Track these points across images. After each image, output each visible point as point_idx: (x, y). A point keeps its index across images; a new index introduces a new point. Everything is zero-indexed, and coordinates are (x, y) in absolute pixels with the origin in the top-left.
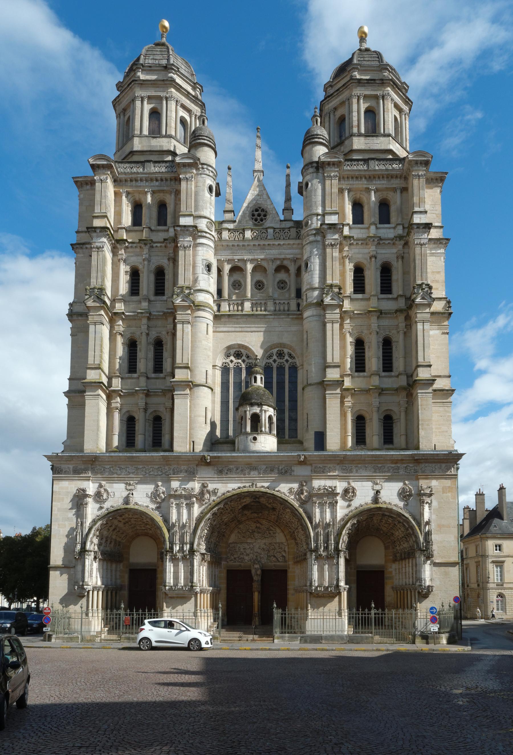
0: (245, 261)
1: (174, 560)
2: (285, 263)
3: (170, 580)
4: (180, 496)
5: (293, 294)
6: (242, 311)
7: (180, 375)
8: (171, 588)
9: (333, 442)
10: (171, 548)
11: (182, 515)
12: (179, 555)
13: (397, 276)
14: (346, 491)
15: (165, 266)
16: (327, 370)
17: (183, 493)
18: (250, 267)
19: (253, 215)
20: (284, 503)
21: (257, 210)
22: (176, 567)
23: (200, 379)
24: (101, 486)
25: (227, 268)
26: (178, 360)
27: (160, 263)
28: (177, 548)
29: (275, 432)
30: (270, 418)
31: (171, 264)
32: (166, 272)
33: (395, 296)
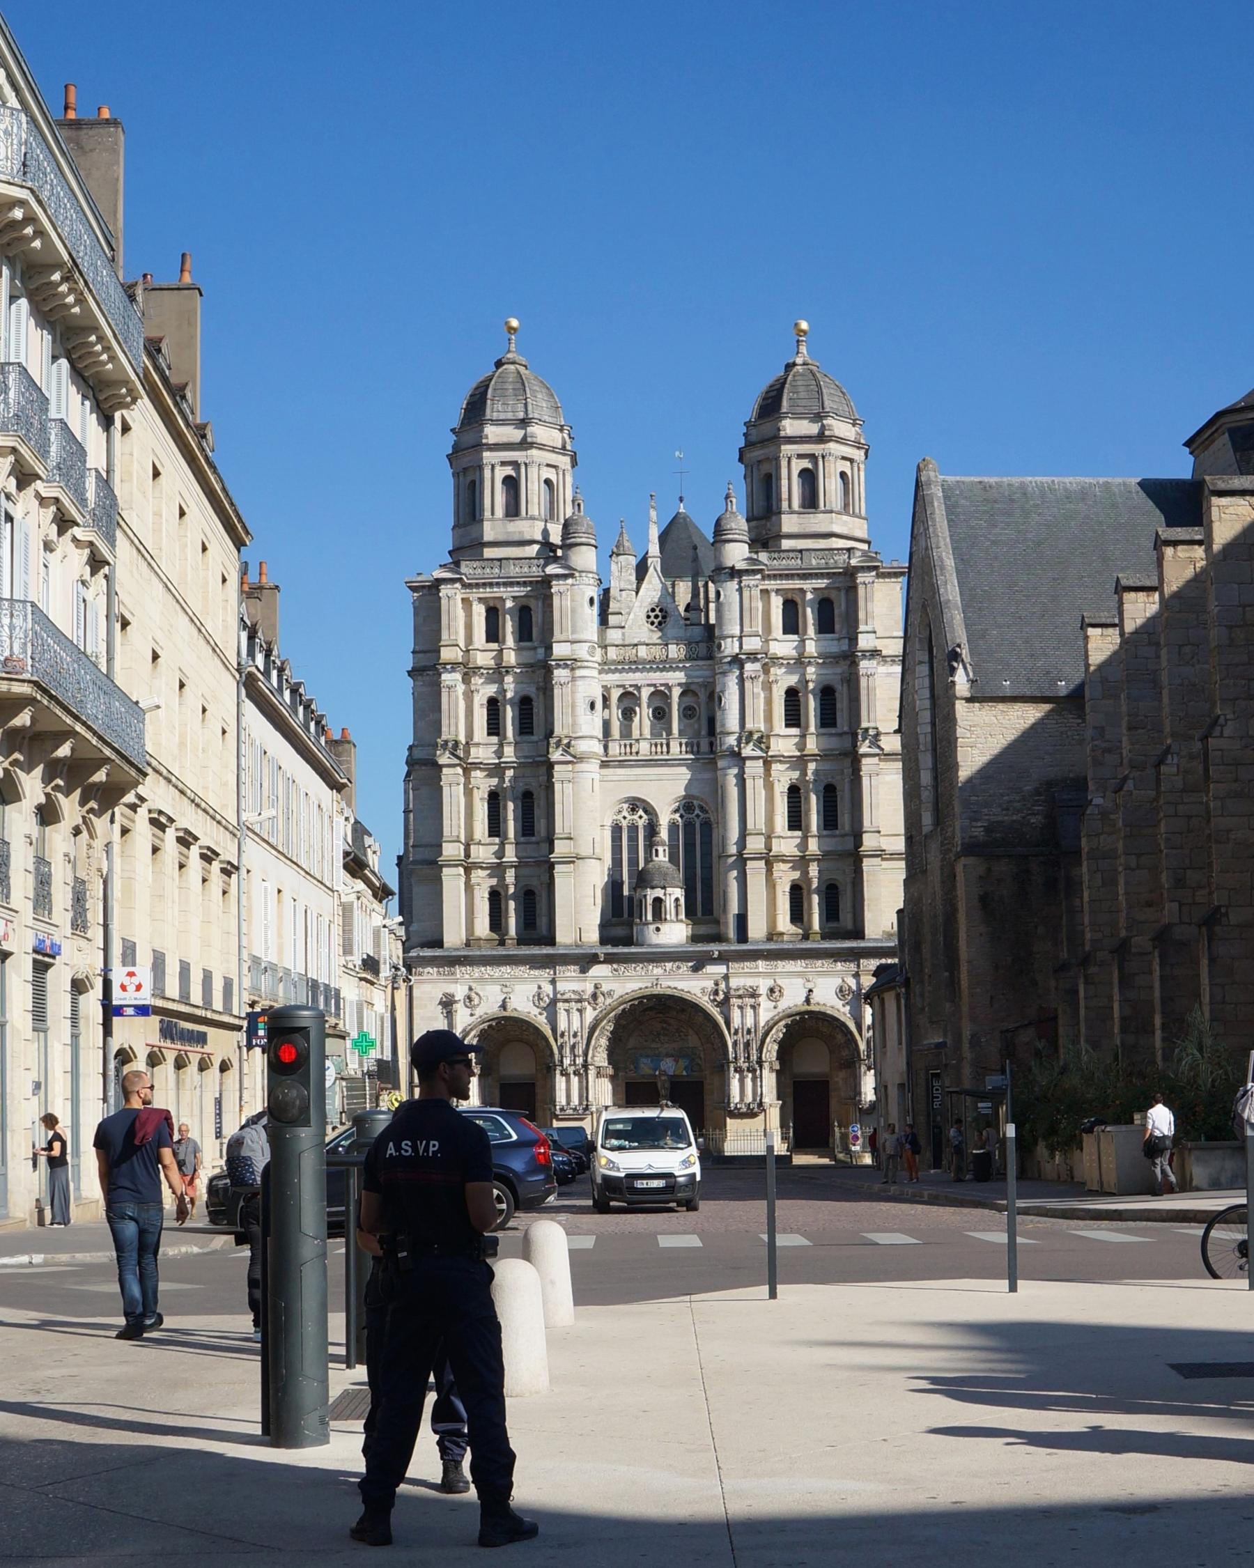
0: (638, 688)
1: (565, 1073)
2: (693, 687)
3: (561, 1098)
4: (566, 1001)
5: (704, 732)
6: (637, 753)
7: (561, 848)
8: (562, 1109)
9: (757, 929)
10: (562, 1062)
11: (572, 1022)
12: (571, 1070)
13: (842, 705)
14: (772, 990)
15: (533, 696)
16: (748, 838)
17: (573, 996)
18: (645, 693)
19: (648, 617)
20: (695, 1008)
21: (653, 610)
22: (568, 1081)
23: (585, 850)
24: (470, 989)
25: (615, 694)
26: (558, 829)
27: (525, 693)
28: (567, 1061)
29: (682, 916)
30: (677, 900)
31: (541, 696)
32: (535, 704)
33: (838, 730)
